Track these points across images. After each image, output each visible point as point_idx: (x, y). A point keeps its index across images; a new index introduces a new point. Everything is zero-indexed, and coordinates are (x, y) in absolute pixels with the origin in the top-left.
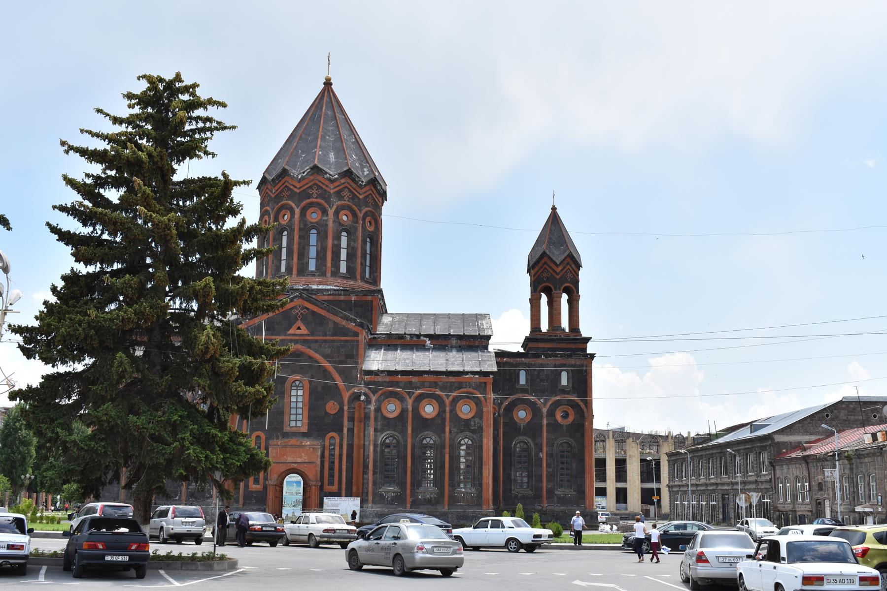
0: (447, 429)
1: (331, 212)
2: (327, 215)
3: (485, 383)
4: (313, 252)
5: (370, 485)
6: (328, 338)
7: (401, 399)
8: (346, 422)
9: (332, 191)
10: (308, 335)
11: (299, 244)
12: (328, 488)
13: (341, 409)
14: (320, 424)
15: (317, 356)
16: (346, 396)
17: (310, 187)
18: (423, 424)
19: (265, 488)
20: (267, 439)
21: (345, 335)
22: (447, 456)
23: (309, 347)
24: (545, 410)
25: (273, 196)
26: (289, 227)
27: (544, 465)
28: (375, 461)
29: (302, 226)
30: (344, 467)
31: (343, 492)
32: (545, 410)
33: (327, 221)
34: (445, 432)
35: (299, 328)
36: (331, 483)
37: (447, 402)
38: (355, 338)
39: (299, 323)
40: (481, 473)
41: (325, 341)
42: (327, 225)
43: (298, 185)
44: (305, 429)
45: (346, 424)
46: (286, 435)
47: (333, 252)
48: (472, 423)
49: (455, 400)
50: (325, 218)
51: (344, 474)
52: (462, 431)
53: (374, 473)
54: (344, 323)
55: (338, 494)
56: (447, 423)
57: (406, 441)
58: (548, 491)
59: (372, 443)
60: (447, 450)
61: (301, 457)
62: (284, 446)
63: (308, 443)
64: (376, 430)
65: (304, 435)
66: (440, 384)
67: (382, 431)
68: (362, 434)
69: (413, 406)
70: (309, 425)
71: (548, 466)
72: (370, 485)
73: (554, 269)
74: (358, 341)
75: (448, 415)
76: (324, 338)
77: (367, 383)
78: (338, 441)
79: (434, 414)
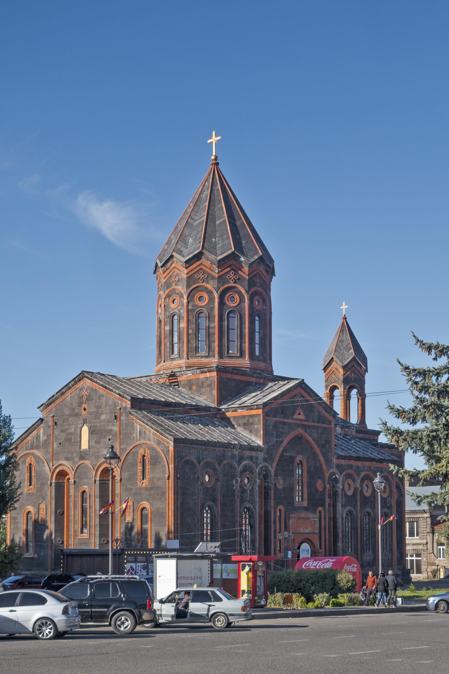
6: (316, 424)
7: (354, 481)
10: (304, 420)
13: (325, 487)
14: (315, 502)
15: (311, 440)
16: (327, 475)
20: (285, 512)
21: (324, 423)
23: (306, 431)
28: (343, 532)
29: (251, 313)
30: (327, 537)
35: (299, 414)
38: (329, 426)
39: (299, 410)
41: (314, 427)
45: (327, 501)
46: (297, 509)
48: (387, 501)
50: (265, 307)
51: (327, 542)
53: (343, 542)
54: (324, 412)
57: (357, 515)
61: (307, 528)
62: (299, 519)
63: (310, 515)
64: (342, 506)
65: (306, 509)
66: (372, 468)
70: (309, 500)
74: (331, 428)
77: (338, 466)
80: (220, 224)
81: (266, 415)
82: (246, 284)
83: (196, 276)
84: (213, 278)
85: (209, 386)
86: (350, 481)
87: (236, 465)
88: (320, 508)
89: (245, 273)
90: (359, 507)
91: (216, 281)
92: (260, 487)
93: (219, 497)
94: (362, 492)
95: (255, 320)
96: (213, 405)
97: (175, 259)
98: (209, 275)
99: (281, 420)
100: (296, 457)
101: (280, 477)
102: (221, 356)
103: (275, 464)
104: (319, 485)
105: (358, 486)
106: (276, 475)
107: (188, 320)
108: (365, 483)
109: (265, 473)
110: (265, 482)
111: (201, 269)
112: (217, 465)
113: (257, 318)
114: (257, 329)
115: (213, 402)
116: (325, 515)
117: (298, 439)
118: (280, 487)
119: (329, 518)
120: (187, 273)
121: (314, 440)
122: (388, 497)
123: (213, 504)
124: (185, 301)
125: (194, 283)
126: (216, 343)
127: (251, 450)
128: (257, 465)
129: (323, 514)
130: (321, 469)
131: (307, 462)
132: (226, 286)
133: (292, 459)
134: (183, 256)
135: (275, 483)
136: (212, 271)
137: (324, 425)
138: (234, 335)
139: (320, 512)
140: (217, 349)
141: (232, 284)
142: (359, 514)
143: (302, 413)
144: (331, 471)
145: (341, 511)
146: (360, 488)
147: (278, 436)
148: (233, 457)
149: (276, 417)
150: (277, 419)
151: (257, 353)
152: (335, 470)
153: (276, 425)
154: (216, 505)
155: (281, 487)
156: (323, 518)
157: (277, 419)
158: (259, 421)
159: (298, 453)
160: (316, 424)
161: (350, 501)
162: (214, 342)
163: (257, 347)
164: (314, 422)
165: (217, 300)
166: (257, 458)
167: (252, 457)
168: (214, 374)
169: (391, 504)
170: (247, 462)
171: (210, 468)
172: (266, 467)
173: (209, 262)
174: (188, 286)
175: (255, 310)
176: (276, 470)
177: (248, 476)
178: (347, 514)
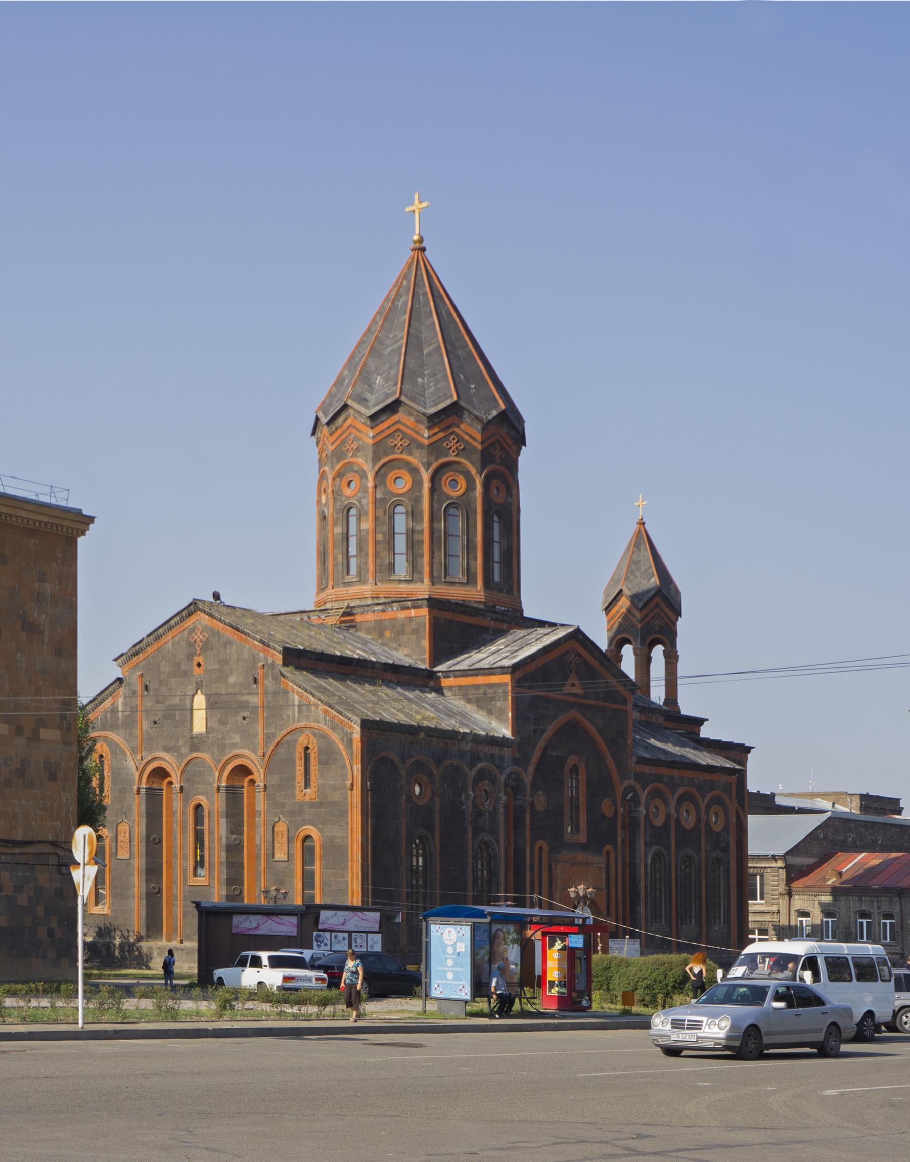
0: (703, 844)
6: (601, 703)
7: (665, 801)
13: (616, 810)
14: (600, 835)
15: (592, 729)
16: (620, 791)
22: (704, 881)
23: (584, 715)
25: (426, 442)
26: (463, 504)
37: (703, 805)
53: (646, 905)
64: (646, 845)
74: (626, 711)
77: (639, 777)
80: (430, 354)
81: (518, 684)
82: (477, 457)
83: (390, 442)
84: (420, 446)
85: (416, 631)
86: (658, 802)
87: (466, 769)
88: (608, 847)
89: (475, 439)
90: (673, 848)
91: (425, 452)
92: (506, 806)
93: (437, 823)
94: (678, 820)
95: (493, 521)
96: (424, 666)
97: (351, 411)
98: (413, 440)
101: (540, 792)
102: (433, 583)
103: (531, 769)
104: (606, 807)
105: (673, 812)
106: (534, 787)
107: (376, 518)
108: (685, 805)
109: (515, 784)
110: (515, 799)
111: (398, 430)
113: (496, 518)
114: (497, 537)
115: (423, 660)
116: (616, 858)
117: (572, 727)
118: (540, 808)
119: (624, 864)
120: (374, 437)
121: (599, 730)
124: (370, 484)
125: (386, 455)
126: (426, 559)
127: (492, 745)
128: (501, 768)
129: (612, 856)
132: (443, 460)
134: (367, 408)
135: (533, 802)
136: (417, 433)
137: (615, 706)
138: (457, 546)
139: (608, 853)
140: (426, 569)
141: (452, 458)
142: (673, 859)
143: (577, 682)
144: (626, 783)
145: (644, 854)
146: (676, 815)
148: (461, 754)
151: (497, 578)
152: (632, 782)
154: (433, 835)
155: (543, 809)
156: (612, 863)
158: (505, 693)
160: (601, 703)
161: (659, 835)
162: (422, 556)
163: (497, 567)
165: (426, 485)
166: (502, 758)
167: (493, 755)
168: (424, 612)
169: (728, 844)
170: (486, 764)
173: (412, 419)
174: (375, 459)
176: (534, 780)
177: (486, 788)
178: (653, 858)
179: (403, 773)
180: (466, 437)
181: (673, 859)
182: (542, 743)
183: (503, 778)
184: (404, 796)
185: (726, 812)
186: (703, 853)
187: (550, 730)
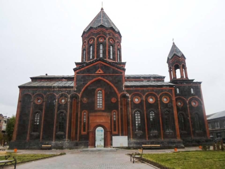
0: (159, 107)
1: (107, 39)
2: (106, 40)
3: (172, 90)
4: (101, 51)
5: (131, 131)
6: (111, 74)
7: (141, 96)
8: (119, 106)
9: (107, 33)
11: (97, 49)
12: (114, 132)
13: (117, 101)
14: (109, 107)
16: (119, 95)
17: (100, 32)
18: (150, 106)
19: (88, 133)
21: (117, 73)
23: (104, 78)
24: (187, 102)
26: (93, 45)
27: (190, 122)
29: (97, 43)
31: (120, 134)
32: (187, 102)
33: (106, 42)
34: (158, 108)
35: (100, 71)
36: (115, 130)
37: (158, 97)
38: (121, 74)
39: (100, 69)
40: (174, 124)
41: (110, 76)
42: (106, 43)
43: (96, 31)
44: (103, 109)
47: (108, 51)
48: (169, 105)
49: (161, 97)
52: (165, 108)
54: (116, 69)
55: (118, 135)
56: (159, 105)
58: (193, 131)
59: (130, 113)
60: (160, 116)
62: (96, 116)
63: (105, 114)
64: (131, 109)
66: (155, 90)
67: (134, 109)
68: (126, 111)
69: (145, 99)
70: (105, 107)
71: (191, 122)
72: (131, 131)
73: (176, 61)
75: (159, 102)
76: (109, 74)
78: (117, 113)
79: (154, 102)
93: (44, 107)
99: (87, 75)
100: (96, 89)
106: (82, 97)
112: (43, 94)
117: (99, 81)
121: (110, 81)
122: (169, 103)
123: (40, 111)
130: (115, 92)
131: (105, 90)
133: (94, 90)
135: (81, 101)
142: (145, 112)
147: (84, 81)
148: (54, 91)
149: (83, 74)
150: (85, 74)
153: (83, 77)
154: (42, 112)
157: (85, 74)
159: (98, 87)
164: (110, 73)
171: (40, 97)
172: (75, 94)
175: (100, 42)
179: (33, 97)
180: (93, 32)
181: (145, 112)
182: (86, 86)
183: (69, 96)
184: (32, 103)
185: (170, 97)
186: (160, 109)
187: (89, 83)
